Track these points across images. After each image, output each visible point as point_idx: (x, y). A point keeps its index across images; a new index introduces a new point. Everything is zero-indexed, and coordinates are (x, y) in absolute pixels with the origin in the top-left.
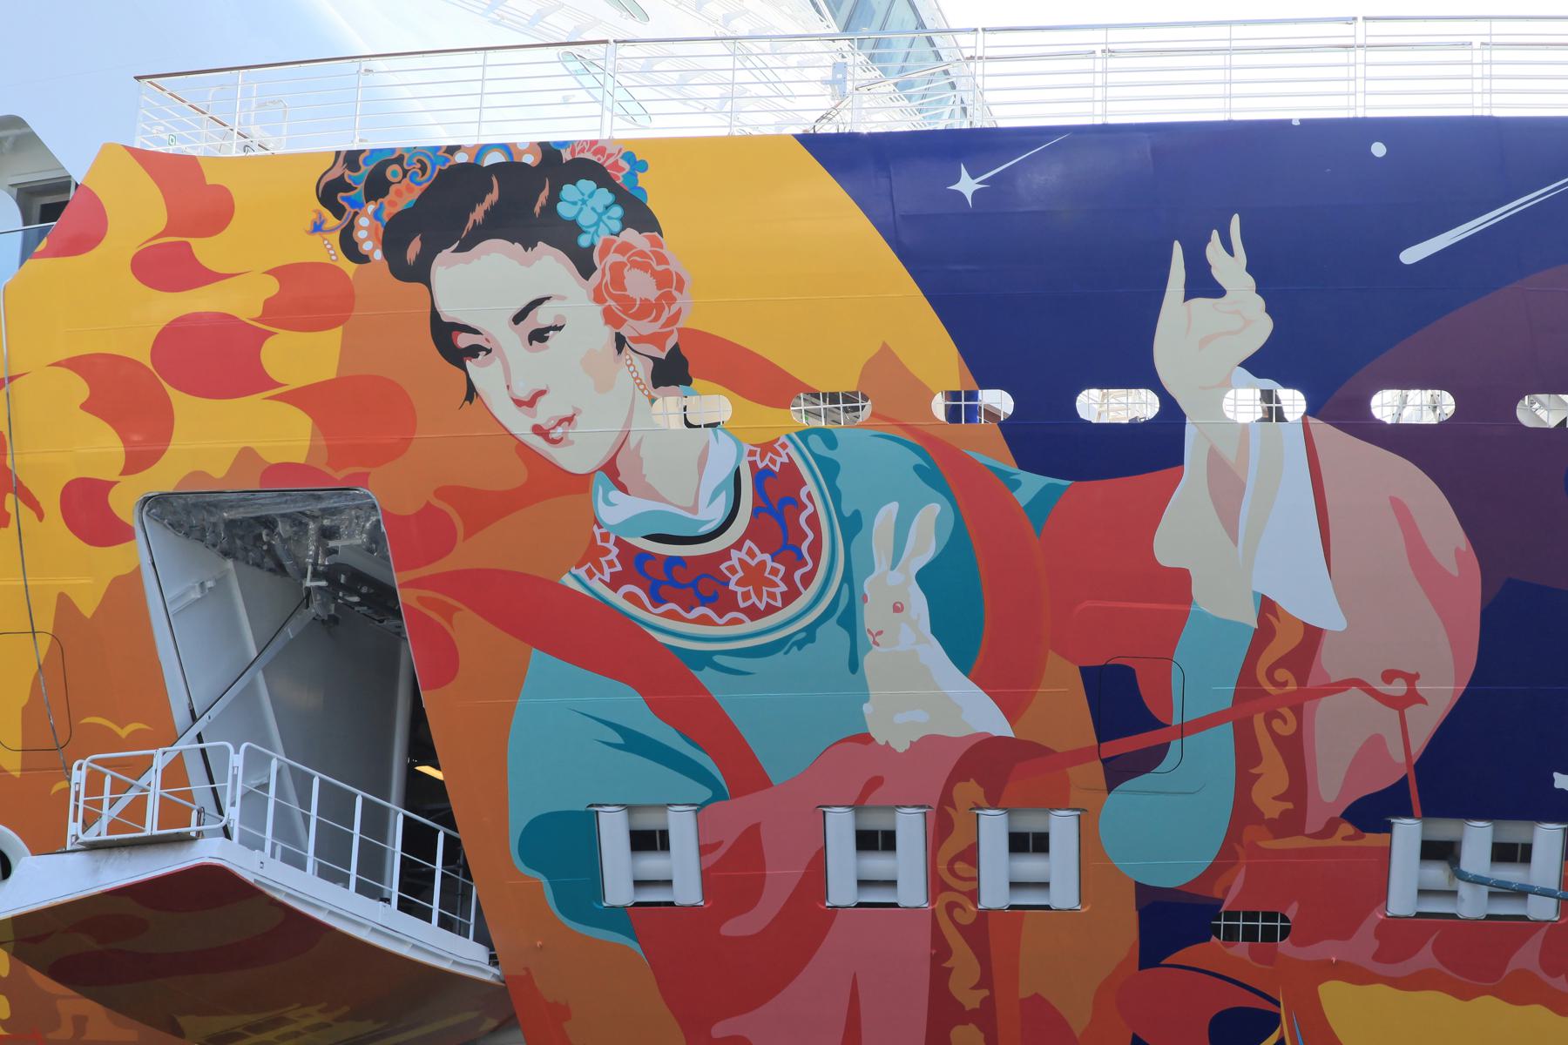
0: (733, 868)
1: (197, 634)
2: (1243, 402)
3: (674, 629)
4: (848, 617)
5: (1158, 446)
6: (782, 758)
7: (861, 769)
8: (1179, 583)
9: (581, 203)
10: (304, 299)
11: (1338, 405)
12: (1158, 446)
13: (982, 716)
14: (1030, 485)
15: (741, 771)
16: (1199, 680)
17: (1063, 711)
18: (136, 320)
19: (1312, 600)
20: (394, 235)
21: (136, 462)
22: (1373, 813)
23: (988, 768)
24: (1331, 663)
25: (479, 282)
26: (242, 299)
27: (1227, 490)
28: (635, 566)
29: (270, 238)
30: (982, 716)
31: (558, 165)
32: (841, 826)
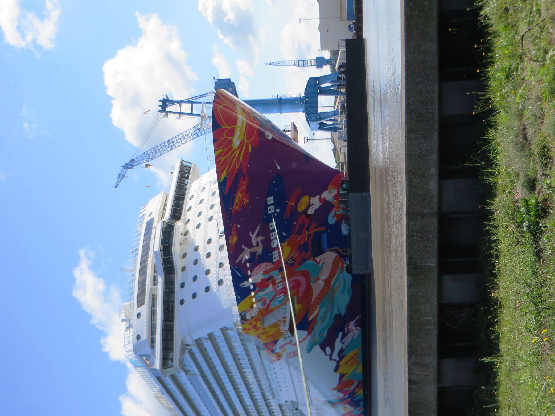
0: (281, 293)
1: (270, 320)
2: (250, 280)
3: (268, 302)
4: (266, 295)
5: (254, 284)
6: (274, 294)
7: (275, 289)
8: (262, 280)
9: (243, 314)
10: (250, 324)
11: (250, 276)
12: (254, 284)
13: (271, 285)
14: (257, 289)
15: (276, 295)
16: (267, 276)
17: (270, 281)
18: (252, 331)
19: (262, 272)
20: (246, 321)
21: (261, 328)
22: (273, 263)
23: (274, 283)
24: (265, 270)
25: (248, 317)
26: (251, 326)
27: (255, 280)
28: (264, 305)
29: (247, 326)
30: (271, 285)
31: (241, 315)
32: (278, 289)
